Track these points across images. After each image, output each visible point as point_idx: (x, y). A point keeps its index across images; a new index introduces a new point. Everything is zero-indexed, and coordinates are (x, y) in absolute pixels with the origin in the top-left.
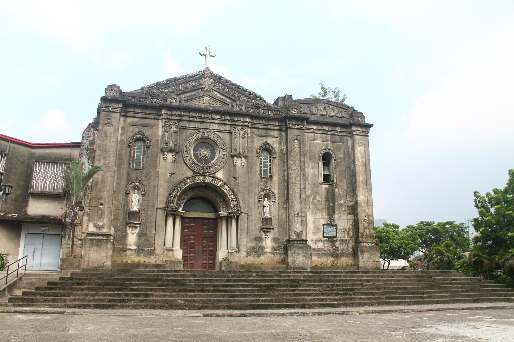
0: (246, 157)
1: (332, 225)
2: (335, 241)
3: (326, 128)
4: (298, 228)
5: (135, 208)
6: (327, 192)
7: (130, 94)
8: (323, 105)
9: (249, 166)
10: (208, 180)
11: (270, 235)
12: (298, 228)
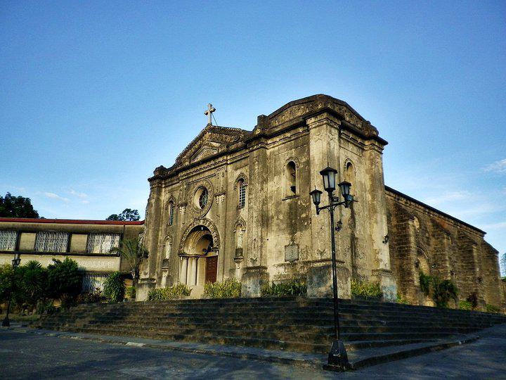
0: (224, 194)
1: (293, 244)
2: (296, 264)
3: (288, 135)
4: (254, 254)
5: (167, 257)
6: (291, 208)
7: (171, 169)
8: (289, 110)
9: (226, 202)
10: (201, 224)
11: (241, 265)
12: (254, 254)
